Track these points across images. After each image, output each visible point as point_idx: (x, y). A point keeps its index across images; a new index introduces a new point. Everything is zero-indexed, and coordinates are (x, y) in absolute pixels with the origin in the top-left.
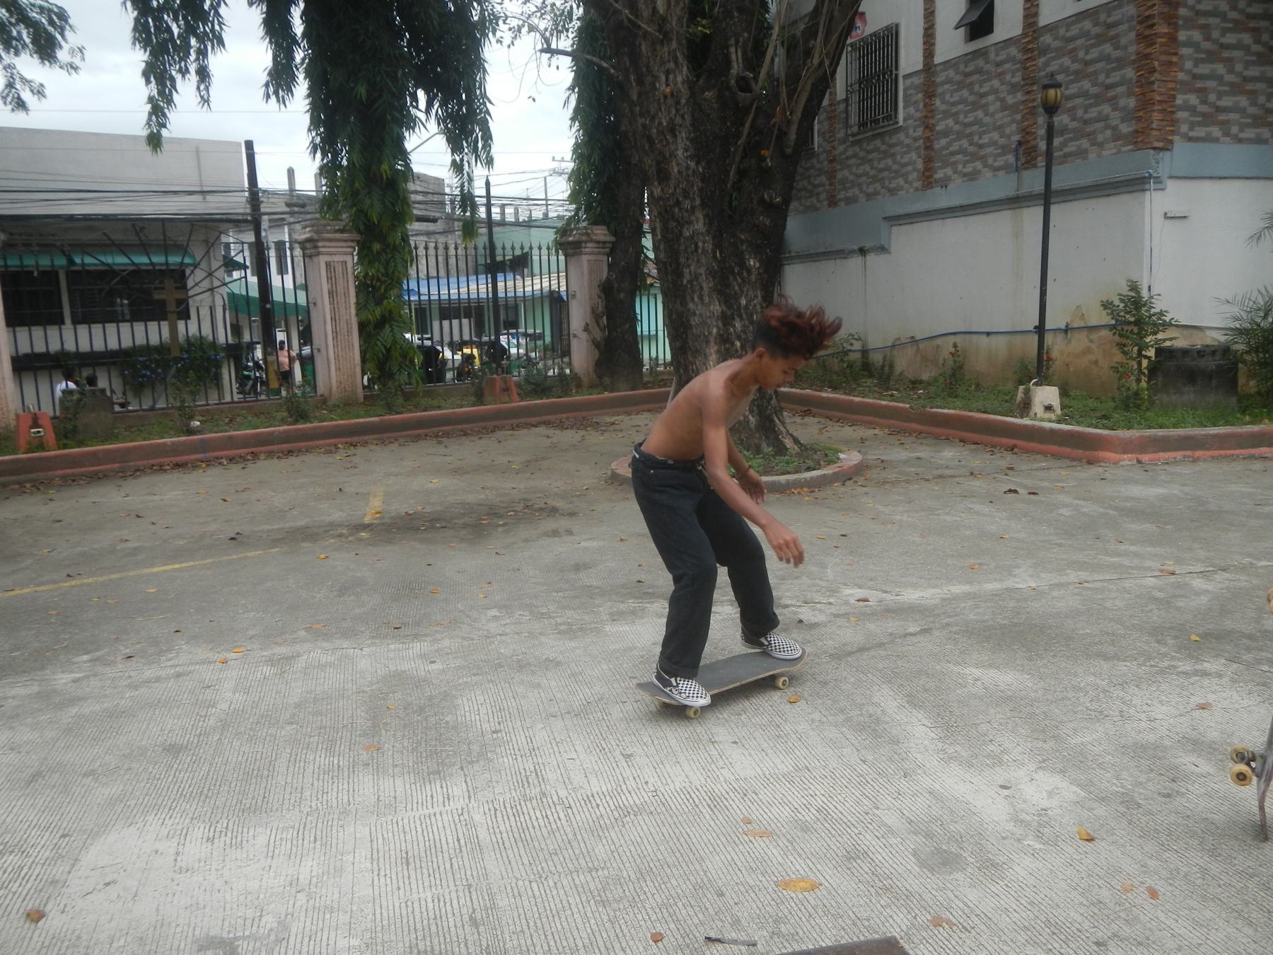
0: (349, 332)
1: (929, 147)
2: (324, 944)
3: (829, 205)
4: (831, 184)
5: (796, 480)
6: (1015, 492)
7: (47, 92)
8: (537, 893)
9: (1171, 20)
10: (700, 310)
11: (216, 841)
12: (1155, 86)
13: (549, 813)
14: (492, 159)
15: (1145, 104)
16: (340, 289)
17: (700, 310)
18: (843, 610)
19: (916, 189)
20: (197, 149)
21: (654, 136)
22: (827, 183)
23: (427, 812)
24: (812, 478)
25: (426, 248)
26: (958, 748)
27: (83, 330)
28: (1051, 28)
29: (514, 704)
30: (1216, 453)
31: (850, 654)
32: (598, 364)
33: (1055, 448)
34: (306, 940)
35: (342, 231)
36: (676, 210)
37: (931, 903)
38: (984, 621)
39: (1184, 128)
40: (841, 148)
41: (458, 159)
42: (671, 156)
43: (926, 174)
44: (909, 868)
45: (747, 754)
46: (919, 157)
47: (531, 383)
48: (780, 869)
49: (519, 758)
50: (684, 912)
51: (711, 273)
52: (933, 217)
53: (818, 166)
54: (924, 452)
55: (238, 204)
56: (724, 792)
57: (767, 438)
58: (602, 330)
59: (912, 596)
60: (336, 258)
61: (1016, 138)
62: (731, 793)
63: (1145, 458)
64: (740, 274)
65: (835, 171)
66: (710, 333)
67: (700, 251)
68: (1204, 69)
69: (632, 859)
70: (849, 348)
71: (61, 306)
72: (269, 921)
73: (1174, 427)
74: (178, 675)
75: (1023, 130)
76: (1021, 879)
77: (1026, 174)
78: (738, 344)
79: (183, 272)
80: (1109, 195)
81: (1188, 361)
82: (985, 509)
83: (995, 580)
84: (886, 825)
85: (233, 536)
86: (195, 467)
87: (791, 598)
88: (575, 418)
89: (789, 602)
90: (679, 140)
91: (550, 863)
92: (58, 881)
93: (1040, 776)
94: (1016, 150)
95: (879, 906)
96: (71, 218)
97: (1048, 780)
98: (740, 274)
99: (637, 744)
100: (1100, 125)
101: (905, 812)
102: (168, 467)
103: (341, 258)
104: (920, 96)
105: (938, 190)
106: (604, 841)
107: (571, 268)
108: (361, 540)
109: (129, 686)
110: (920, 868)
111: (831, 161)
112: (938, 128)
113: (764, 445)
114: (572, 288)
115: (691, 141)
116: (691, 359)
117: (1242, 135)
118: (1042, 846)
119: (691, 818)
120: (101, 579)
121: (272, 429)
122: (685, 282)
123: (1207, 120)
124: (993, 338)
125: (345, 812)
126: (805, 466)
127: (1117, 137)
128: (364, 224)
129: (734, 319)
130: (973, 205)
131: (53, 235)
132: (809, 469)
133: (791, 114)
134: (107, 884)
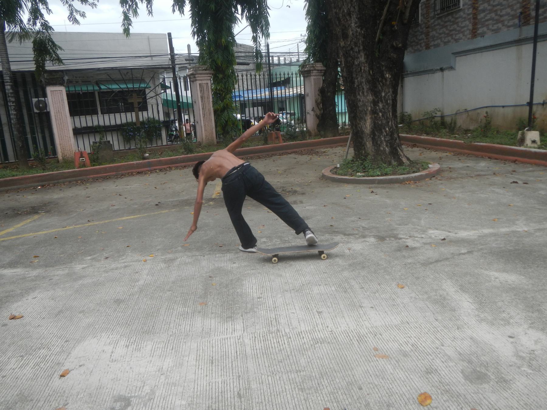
0: (210, 114)
1: (475, 18)
2: (170, 402)
3: (426, 49)
4: (427, 39)
5: (408, 177)
6: (516, 182)
7: (86, 15)
8: (270, 382)
10: (362, 99)
11: (130, 347)
13: (280, 340)
14: (269, 34)
16: (206, 95)
17: (362, 99)
18: (429, 241)
19: (469, 39)
20: (148, 38)
21: (341, 17)
22: (425, 38)
23: (224, 337)
24: (415, 176)
25: (247, 76)
26: (486, 315)
27: (106, 116)
29: (269, 285)
31: (431, 263)
32: (318, 126)
33: (537, 161)
34: (162, 399)
35: (206, 70)
36: (351, 52)
37: (470, 400)
38: (500, 248)
40: (432, 21)
41: (255, 35)
42: (348, 26)
43: (474, 31)
44: (459, 379)
45: (377, 314)
46: (470, 23)
47: (289, 135)
48: (392, 376)
49: (269, 311)
50: (341, 397)
51: (368, 81)
52: (477, 52)
53: (421, 30)
54: (470, 163)
55: (165, 61)
56: (365, 333)
57: (394, 158)
58: (320, 110)
59: (463, 234)
61: (520, 10)
62: (369, 334)
65: (429, 32)
66: (367, 109)
67: (362, 71)
69: (317, 367)
70: (435, 115)
72: (147, 389)
74: (126, 267)
75: (523, 7)
76: (520, 390)
77: (524, 28)
78: (381, 114)
79: (145, 91)
82: (501, 191)
83: (506, 227)
84: (447, 355)
85: (157, 203)
86: (145, 174)
87: (403, 235)
88: (308, 150)
89: (402, 236)
90: (352, 19)
91: (278, 367)
92: (60, 363)
93: (531, 332)
94: (519, 17)
95: (442, 401)
96: (99, 69)
97: (535, 334)
99: (324, 306)
101: (458, 348)
102: (134, 174)
105: (479, 38)
106: (305, 357)
107: (306, 82)
108: (210, 205)
109: (104, 271)
110: (465, 380)
111: (427, 28)
112: (481, 8)
113: (393, 161)
114: (307, 91)
116: (358, 122)
118: (531, 371)
119: (348, 346)
120: (102, 222)
121: (177, 157)
122: (355, 86)
124: (506, 109)
125: (187, 335)
126: (412, 171)
128: (215, 66)
129: (378, 102)
130: (496, 45)
131: (93, 77)
132: (414, 172)
133: (407, 3)
134: (80, 366)
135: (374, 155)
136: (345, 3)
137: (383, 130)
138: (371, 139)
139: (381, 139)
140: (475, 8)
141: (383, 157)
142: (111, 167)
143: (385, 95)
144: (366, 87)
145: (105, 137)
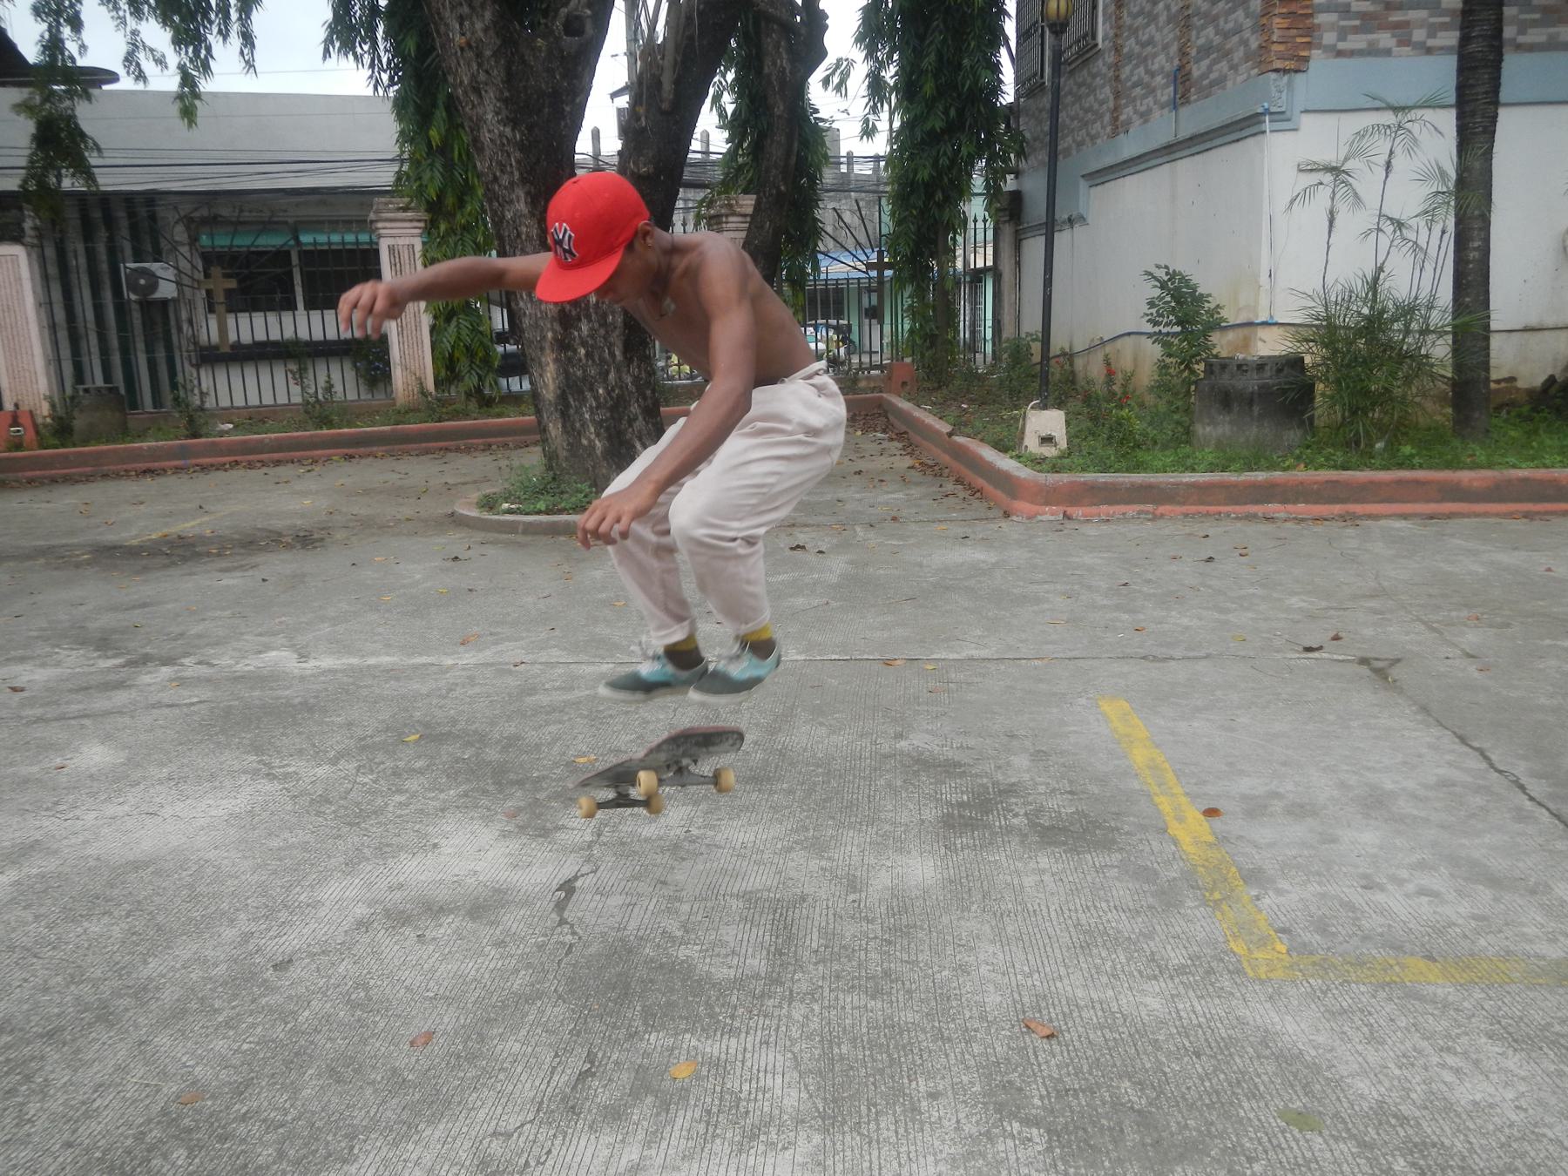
0: (418, 326)
1: (1117, 78)
30: (1193, 509)
35: (405, 209)
39: (1329, 38)
60: (401, 241)
61: (1176, 62)
63: (1077, 512)
66: (544, 338)
67: (524, 237)
71: (293, 291)
73: (1128, 471)
78: (583, 351)
80: (1238, 140)
81: (1225, 380)
100: (1235, 39)
103: (407, 241)
112: (1126, 50)
115: (505, 101)
117: (1431, 43)
127: (1247, 58)
128: (428, 202)
129: (580, 320)
133: (663, 58)
135: (566, 459)
136: (462, 63)
137: (588, 395)
139: (582, 415)
140: (1117, 49)
141: (589, 464)
142: (80, 453)
143: (597, 302)
145: (311, 371)
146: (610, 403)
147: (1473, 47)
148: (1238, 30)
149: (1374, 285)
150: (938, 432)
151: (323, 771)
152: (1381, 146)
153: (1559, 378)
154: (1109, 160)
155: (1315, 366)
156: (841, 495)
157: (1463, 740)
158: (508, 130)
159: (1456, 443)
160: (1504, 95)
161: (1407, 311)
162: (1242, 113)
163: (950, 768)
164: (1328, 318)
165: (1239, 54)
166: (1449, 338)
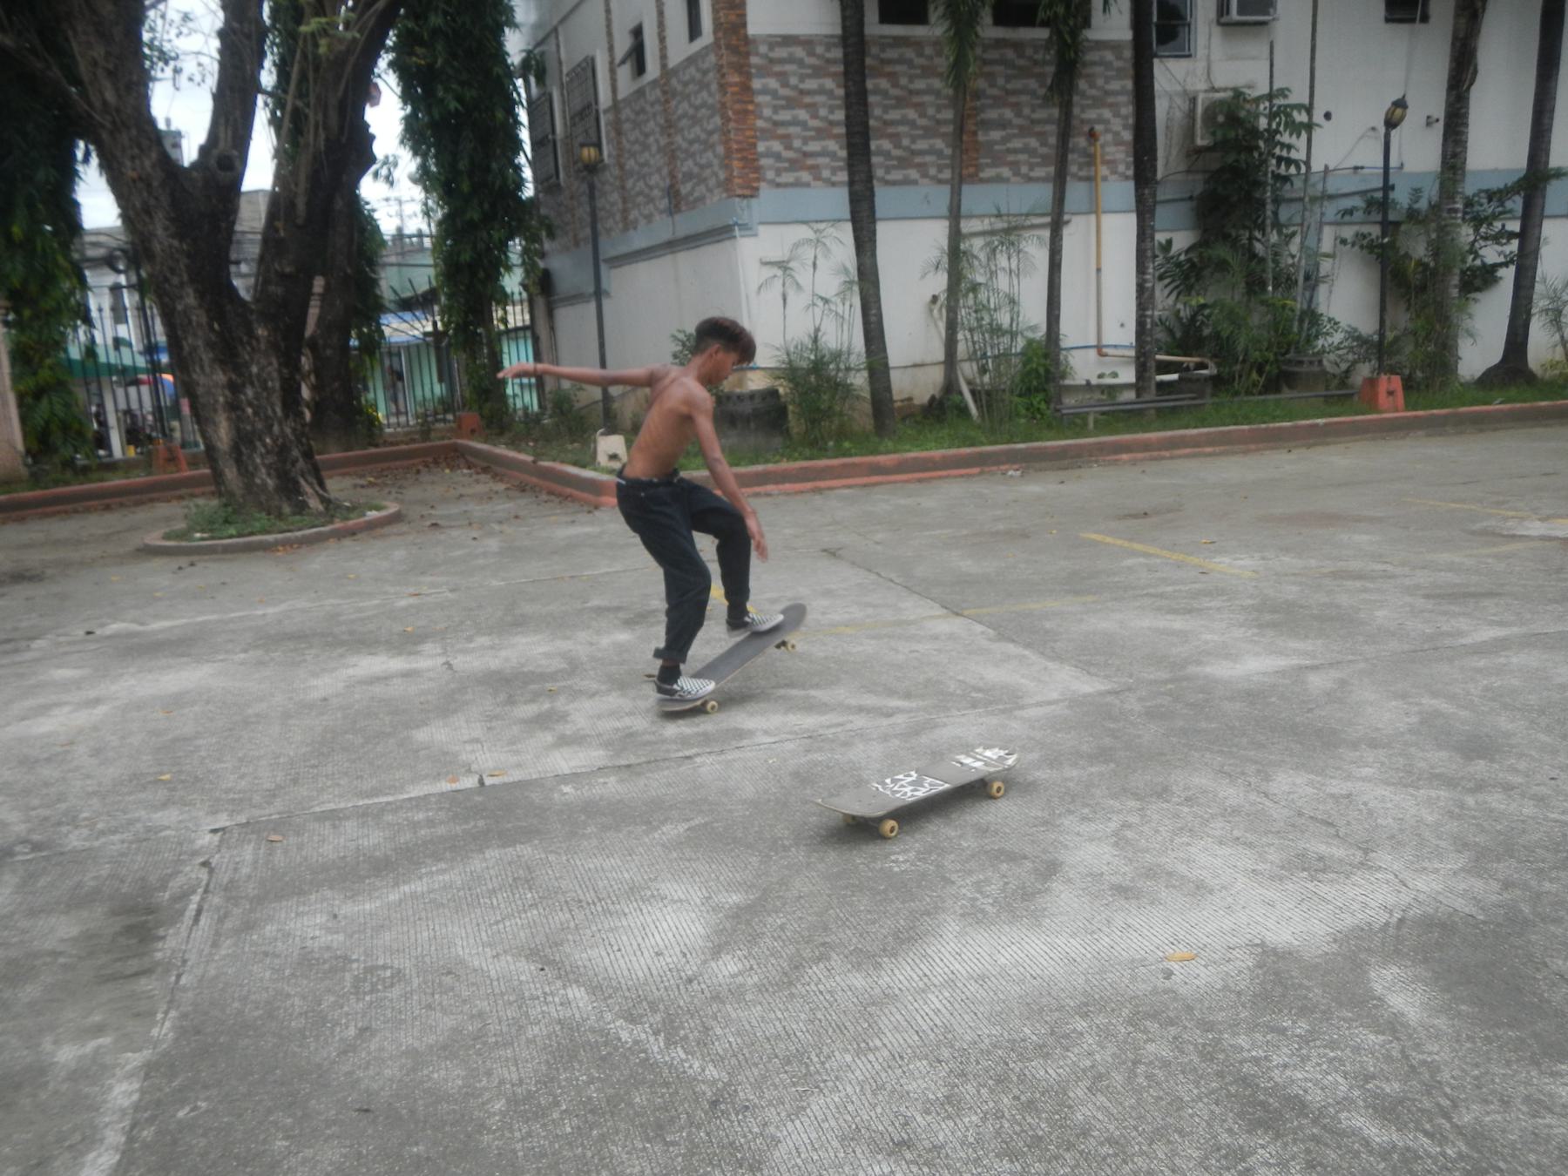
1: (623, 188)
9: (742, 69)
10: (202, 380)
12: (732, 136)
15: (729, 154)
24: (303, 536)
28: (675, 72)
33: (585, 495)
36: (167, 286)
39: (770, 175)
51: (210, 345)
57: (289, 499)
59: (156, 625)
61: (668, 182)
64: (250, 344)
66: (216, 401)
68: (785, 116)
77: (677, 217)
78: (250, 411)
94: (669, 194)
98: (250, 344)
104: (613, 134)
105: (631, 232)
112: (627, 167)
123: (794, 165)
127: (719, 185)
129: (244, 385)
133: (296, 185)
137: (258, 444)
138: (231, 462)
139: (254, 461)
140: (621, 167)
144: (206, 356)
146: (276, 449)
147: (857, 187)
148: (710, 165)
149: (815, 340)
150: (524, 463)
151: (242, 656)
152: (808, 253)
153: (937, 396)
154: (623, 249)
155: (786, 394)
156: (465, 508)
157: (870, 571)
158: (176, 243)
159: (877, 439)
160: (878, 215)
161: (837, 356)
162: (720, 224)
163: (618, 609)
164: (790, 362)
165: (712, 182)
166: (865, 374)
